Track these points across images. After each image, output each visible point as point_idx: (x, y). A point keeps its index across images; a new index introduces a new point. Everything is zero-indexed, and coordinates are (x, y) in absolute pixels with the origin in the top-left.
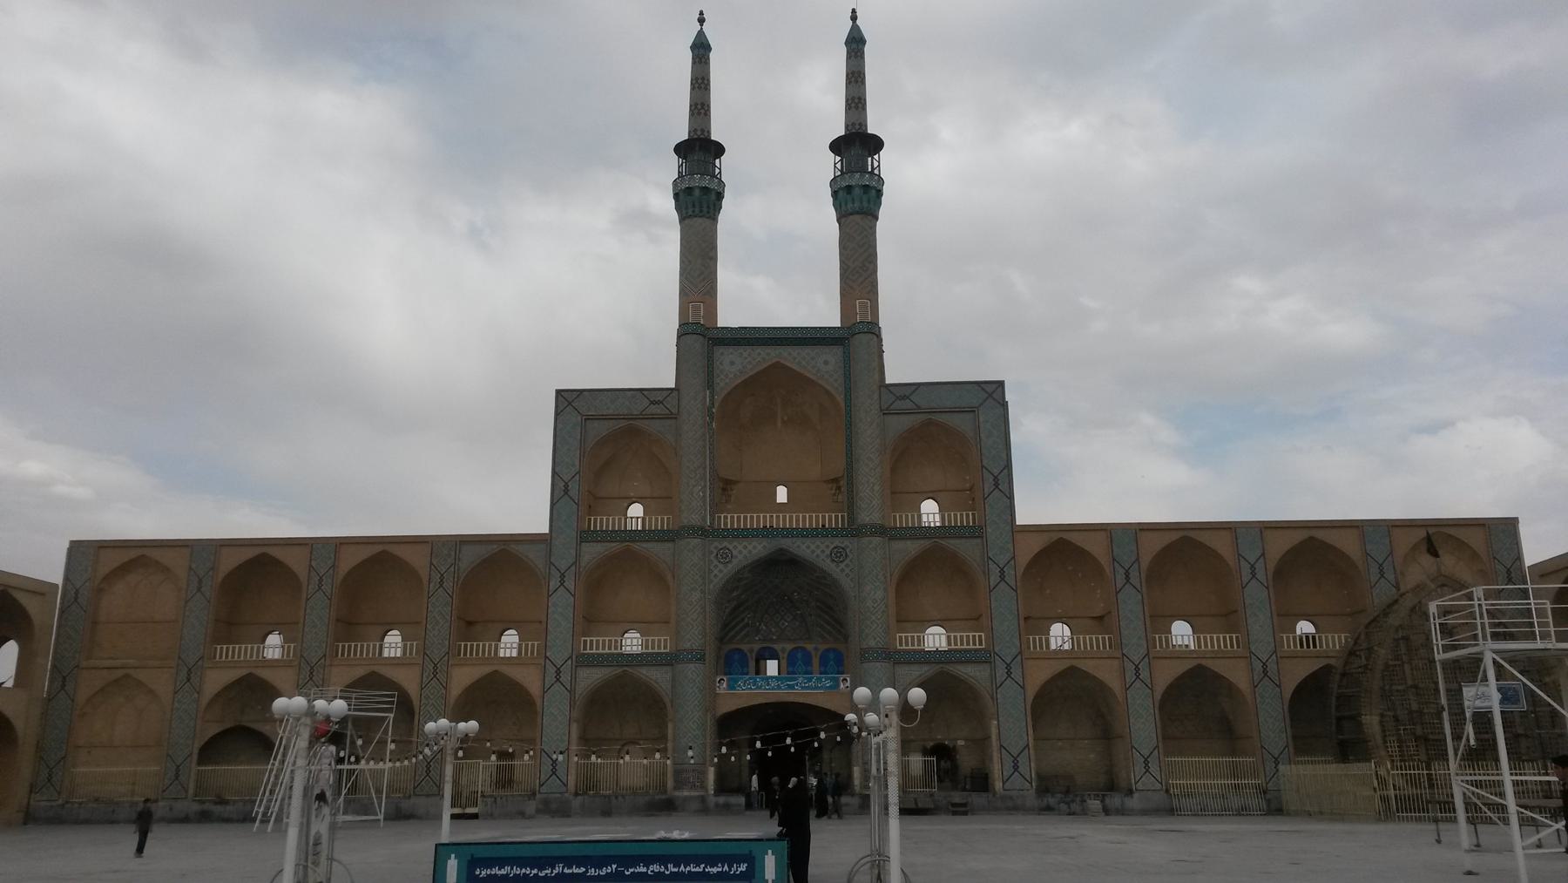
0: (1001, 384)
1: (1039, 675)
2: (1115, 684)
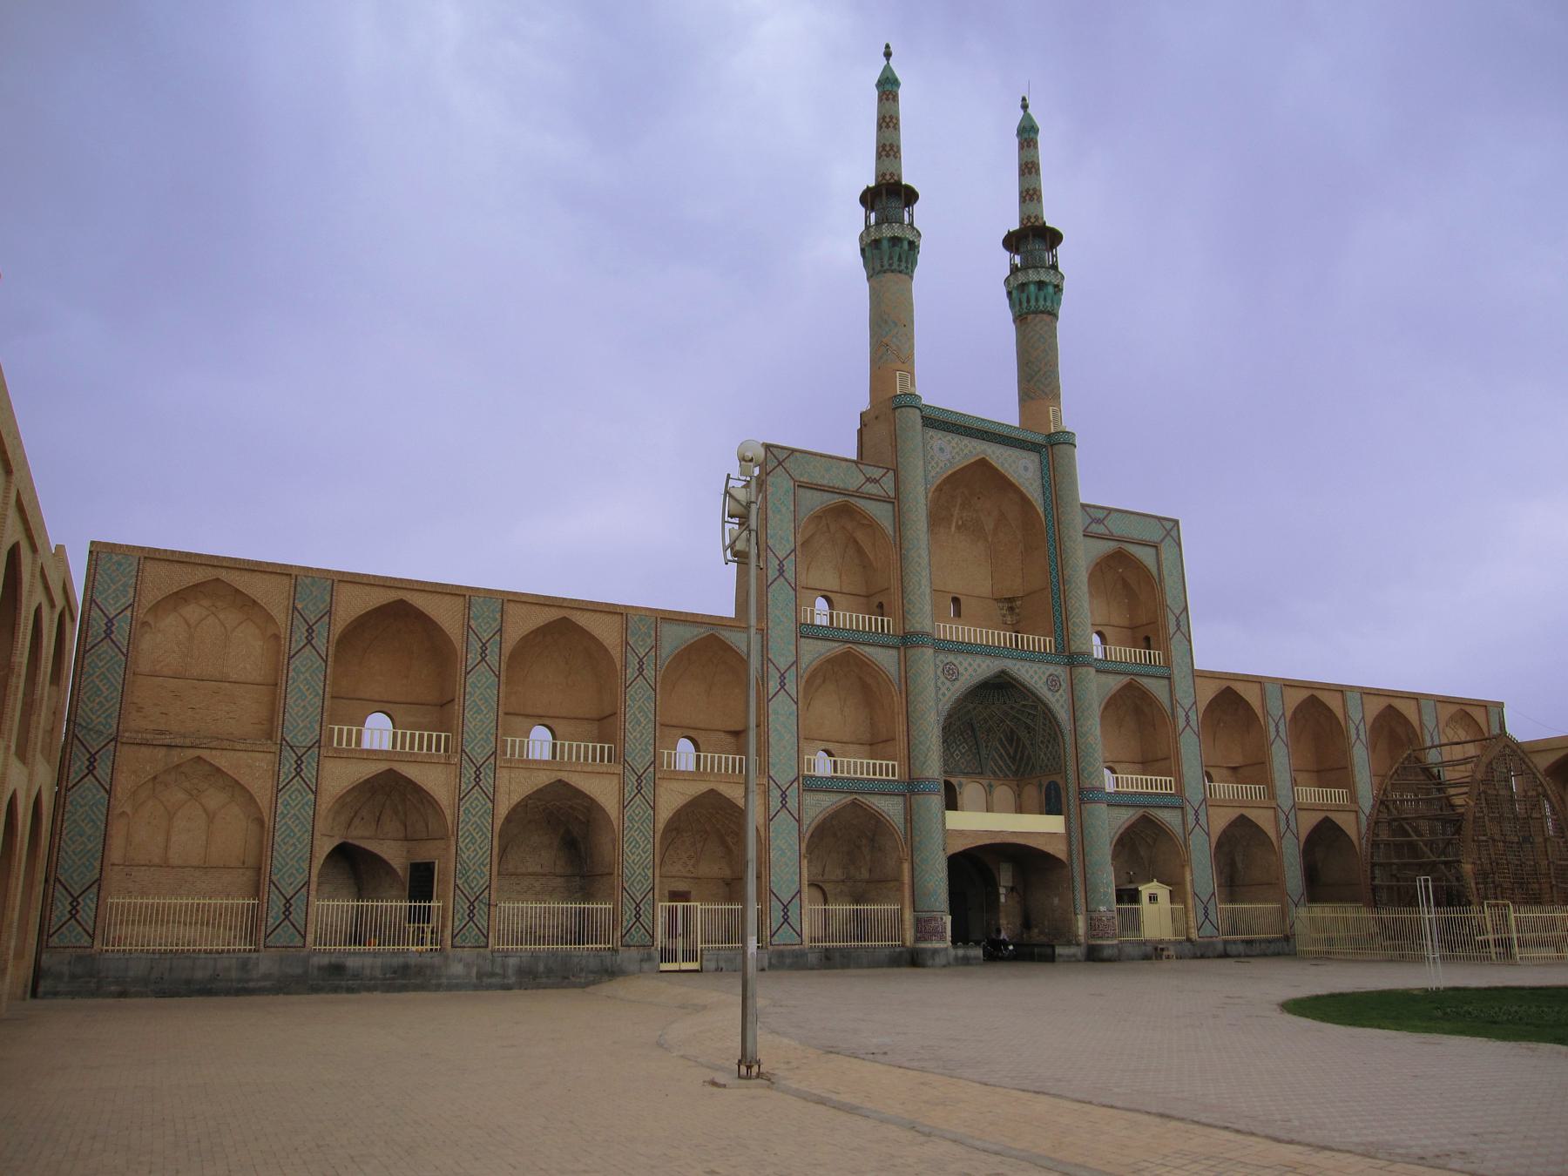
0: (1176, 522)
2: (1272, 834)
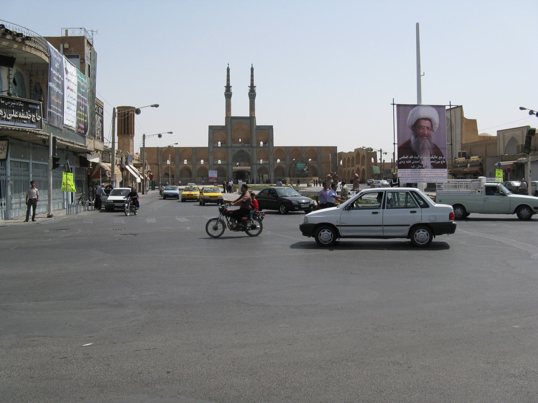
1: (275, 167)
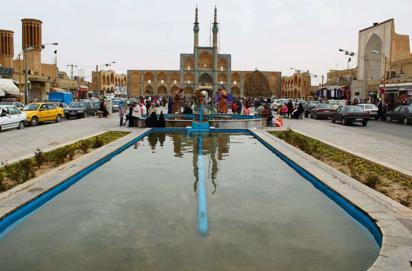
0: (230, 55)
2: (240, 88)
